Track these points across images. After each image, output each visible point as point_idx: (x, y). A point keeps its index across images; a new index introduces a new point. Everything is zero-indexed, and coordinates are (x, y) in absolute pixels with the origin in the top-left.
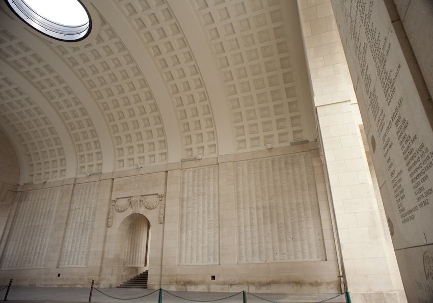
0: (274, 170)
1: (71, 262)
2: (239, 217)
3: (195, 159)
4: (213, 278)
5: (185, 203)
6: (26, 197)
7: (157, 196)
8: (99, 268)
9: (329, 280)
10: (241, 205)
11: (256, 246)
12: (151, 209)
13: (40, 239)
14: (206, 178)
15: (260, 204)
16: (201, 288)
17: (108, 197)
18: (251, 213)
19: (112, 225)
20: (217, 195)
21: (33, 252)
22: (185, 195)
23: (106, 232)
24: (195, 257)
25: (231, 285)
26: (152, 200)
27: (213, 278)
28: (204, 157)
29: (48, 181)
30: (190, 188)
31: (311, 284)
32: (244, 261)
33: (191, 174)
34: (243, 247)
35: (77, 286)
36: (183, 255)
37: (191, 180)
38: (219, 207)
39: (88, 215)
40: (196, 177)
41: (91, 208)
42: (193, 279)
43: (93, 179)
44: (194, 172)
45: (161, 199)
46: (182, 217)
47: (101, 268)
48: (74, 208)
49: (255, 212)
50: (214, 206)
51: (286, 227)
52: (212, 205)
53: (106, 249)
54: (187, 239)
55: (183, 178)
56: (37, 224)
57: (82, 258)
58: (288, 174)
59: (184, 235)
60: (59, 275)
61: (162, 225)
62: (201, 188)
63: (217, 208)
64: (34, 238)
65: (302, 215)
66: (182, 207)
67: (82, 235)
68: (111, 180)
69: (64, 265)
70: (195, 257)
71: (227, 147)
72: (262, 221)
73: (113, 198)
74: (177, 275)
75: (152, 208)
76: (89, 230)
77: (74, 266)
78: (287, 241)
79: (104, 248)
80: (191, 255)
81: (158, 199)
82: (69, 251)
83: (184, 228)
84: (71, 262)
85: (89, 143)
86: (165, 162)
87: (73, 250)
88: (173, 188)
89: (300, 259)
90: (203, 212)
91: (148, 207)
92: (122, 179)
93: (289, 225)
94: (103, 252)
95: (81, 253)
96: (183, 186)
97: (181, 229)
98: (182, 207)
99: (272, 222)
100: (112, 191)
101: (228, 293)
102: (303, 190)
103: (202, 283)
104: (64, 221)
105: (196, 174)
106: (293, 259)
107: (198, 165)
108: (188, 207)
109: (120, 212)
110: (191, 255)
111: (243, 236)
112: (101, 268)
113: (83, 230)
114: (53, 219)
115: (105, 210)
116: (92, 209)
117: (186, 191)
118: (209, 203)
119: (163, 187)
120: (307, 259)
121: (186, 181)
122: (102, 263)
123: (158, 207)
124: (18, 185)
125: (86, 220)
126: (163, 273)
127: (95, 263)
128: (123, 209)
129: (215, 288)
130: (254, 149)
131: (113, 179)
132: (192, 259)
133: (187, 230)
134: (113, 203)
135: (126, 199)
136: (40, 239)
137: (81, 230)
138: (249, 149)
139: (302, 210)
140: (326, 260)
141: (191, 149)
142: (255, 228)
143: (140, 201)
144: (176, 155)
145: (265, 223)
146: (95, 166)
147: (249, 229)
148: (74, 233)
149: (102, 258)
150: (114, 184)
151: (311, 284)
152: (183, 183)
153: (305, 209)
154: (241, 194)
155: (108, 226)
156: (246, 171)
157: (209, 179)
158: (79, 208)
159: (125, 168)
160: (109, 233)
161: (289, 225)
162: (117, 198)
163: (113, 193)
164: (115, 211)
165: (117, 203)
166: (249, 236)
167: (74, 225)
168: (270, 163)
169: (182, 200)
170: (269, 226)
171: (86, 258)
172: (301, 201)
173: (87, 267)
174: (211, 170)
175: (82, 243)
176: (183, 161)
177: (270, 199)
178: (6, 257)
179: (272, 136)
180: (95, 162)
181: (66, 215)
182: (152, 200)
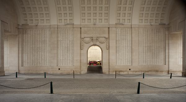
0: (152, 33)
1: (64, 64)
2: (139, 49)
3: (123, 24)
4: (130, 69)
5: (118, 42)
6: (26, 32)
9: (165, 70)
10: (140, 45)
11: (144, 59)
13: (43, 53)
14: (126, 32)
15: (147, 45)
16: (125, 73)
17: (79, 36)
18: (143, 48)
20: (131, 40)
21: (41, 59)
22: (118, 39)
23: (80, 52)
24: (122, 62)
25: (136, 72)
27: (130, 69)
28: (125, 24)
29: (40, 24)
30: (120, 36)
31: (161, 71)
32: (140, 64)
33: (120, 30)
34: (140, 59)
36: (118, 62)
37: (120, 33)
38: (132, 45)
39: (69, 44)
40: (122, 32)
42: (122, 70)
43: (68, 26)
44: (121, 30)
45: (107, 39)
46: (116, 47)
47: (80, 66)
48: (60, 40)
49: (144, 47)
50: (130, 44)
51: (155, 54)
52: (129, 44)
53: (82, 59)
55: (116, 32)
56: (38, 46)
57: (69, 62)
58: (157, 35)
59: (118, 54)
60: (59, 69)
61: (108, 50)
63: (131, 45)
64: (39, 53)
65: (160, 50)
66: (116, 44)
67: (67, 53)
69: (60, 65)
70: (122, 62)
71: (135, 21)
72: (147, 51)
73: (82, 37)
76: (71, 50)
77: (66, 65)
78: (154, 58)
80: (121, 62)
81: (105, 39)
84: (64, 64)
85: (66, 7)
86: (108, 23)
87: (64, 59)
88: (112, 35)
89: (158, 64)
93: (156, 53)
94: (81, 60)
95: (68, 60)
96: (116, 35)
98: (116, 44)
99: (150, 52)
101: (135, 74)
102: (161, 42)
103: (126, 71)
104: (56, 46)
105: (122, 31)
106: (156, 64)
107: (123, 27)
110: (121, 62)
111: (140, 56)
113: (67, 51)
114: (48, 45)
116: (71, 41)
117: (118, 37)
118: (127, 43)
120: (160, 64)
121: (118, 33)
122: (80, 64)
123: (106, 43)
124: (19, 25)
125: (68, 46)
126: (110, 68)
127: (77, 64)
129: (130, 73)
130: (145, 24)
131: (81, 28)
132: (121, 63)
136: (43, 53)
138: (143, 24)
139: (160, 49)
140: (165, 64)
141: (119, 19)
142: (145, 53)
144: (113, 21)
145: (148, 52)
147: (142, 54)
148: (62, 51)
149: (80, 63)
150: (82, 30)
151: (161, 71)
153: (161, 49)
154: (140, 41)
155: (81, 49)
156: (142, 32)
157: (127, 33)
159: (86, 23)
161: (156, 53)
163: (82, 34)
166: (142, 56)
167: (62, 47)
168: (151, 30)
169: (116, 41)
170: (149, 53)
172: (160, 45)
174: (129, 30)
175: (68, 56)
176: (116, 24)
177: (150, 44)
178: (24, 60)
179: (153, 19)
180: (68, 18)
181: (56, 43)
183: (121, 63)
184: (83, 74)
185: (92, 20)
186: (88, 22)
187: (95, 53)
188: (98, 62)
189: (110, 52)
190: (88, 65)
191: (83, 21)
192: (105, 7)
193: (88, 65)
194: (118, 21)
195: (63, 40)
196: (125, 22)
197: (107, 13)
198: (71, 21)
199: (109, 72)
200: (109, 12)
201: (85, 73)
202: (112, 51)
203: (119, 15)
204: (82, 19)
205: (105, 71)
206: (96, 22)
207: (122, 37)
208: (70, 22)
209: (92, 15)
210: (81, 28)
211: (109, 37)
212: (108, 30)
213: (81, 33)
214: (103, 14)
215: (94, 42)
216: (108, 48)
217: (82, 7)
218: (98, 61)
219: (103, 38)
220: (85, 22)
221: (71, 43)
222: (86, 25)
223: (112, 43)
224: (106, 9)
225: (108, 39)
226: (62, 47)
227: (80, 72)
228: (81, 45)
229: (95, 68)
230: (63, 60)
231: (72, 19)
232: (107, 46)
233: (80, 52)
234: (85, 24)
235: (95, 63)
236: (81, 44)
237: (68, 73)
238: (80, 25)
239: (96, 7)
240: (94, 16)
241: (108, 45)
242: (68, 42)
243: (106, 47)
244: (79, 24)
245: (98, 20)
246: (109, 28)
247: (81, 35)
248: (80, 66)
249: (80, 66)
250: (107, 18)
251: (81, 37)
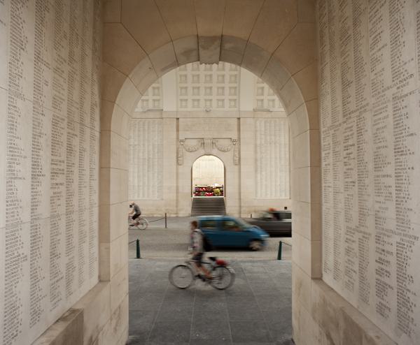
1: (141, 195)
8: (175, 202)
20: (288, 146)
22: (258, 142)
23: (177, 169)
26: (226, 143)
30: (263, 136)
33: (263, 124)
35: (155, 216)
37: (263, 129)
41: (153, 145)
43: (151, 115)
46: (256, 160)
47: (177, 201)
48: (132, 144)
50: (285, 154)
54: (261, 179)
55: (256, 127)
59: (259, 175)
61: (237, 167)
62: (273, 137)
66: (256, 152)
67: (148, 171)
74: (255, 206)
79: (177, 183)
81: (231, 143)
82: (136, 185)
83: (259, 170)
84: (141, 195)
90: (276, 158)
92: (189, 119)
94: (177, 187)
97: (256, 171)
100: (178, 130)
108: (261, 153)
115: (174, 148)
118: (280, 151)
119: (236, 133)
122: (177, 197)
125: (151, 156)
126: (242, 205)
131: (178, 119)
132: (266, 194)
133: (261, 171)
137: (146, 168)
141: (262, 100)
146: (151, 101)
149: (177, 192)
150: (180, 123)
152: (256, 131)
155: (178, 164)
158: (139, 145)
159: (190, 108)
160: (180, 171)
164: (184, 150)
167: (136, 160)
171: (158, 192)
173: (163, 199)
176: (255, 110)
182: (226, 143)
183: (266, 194)
184: (184, 217)
185: (202, 103)
186: (194, 107)
187: (208, 170)
188: (217, 188)
189: (242, 170)
190: (194, 195)
191: (184, 103)
192: (231, 76)
193: (194, 195)
194: (260, 103)
195: (139, 145)
196: (274, 107)
197: (235, 100)
198: (156, 103)
199: (240, 213)
200: (239, 85)
201: (187, 215)
202: (247, 167)
203: (260, 91)
204: (181, 100)
206: (211, 106)
207: (268, 138)
208: (154, 106)
209: (202, 91)
210: (178, 119)
211: (239, 138)
212: (236, 123)
213: (178, 130)
214: (227, 91)
215: (207, 146)
216: (238, 163)
217: (181, 76)
218: (216, 185)
220: (186, 107)
221: (156, 150)
222: (190, 112)
223: (247, 152)
224: (233, 78)
225: (237, 142)
226: (136, 160)
227: (177, 214)
230: (138, 186)
231: (159, 100)
232: (235, 158)
233: (175, 171)
234: (185, 109)
235: (210, 190)
236: (177, 153)
237: (151, 216)
238: (177, 112)
239: (211, 88)
240: (206, 95)
241: (237, 156)
242: (151, 147)
243: (232, 161)
244: (175, 110)
245: (214, 103)
246: (239, 119)
247: (178, 135)
248: (177, 200)
249: (177, 200)
250: (235, 97)
251: (178, 138)
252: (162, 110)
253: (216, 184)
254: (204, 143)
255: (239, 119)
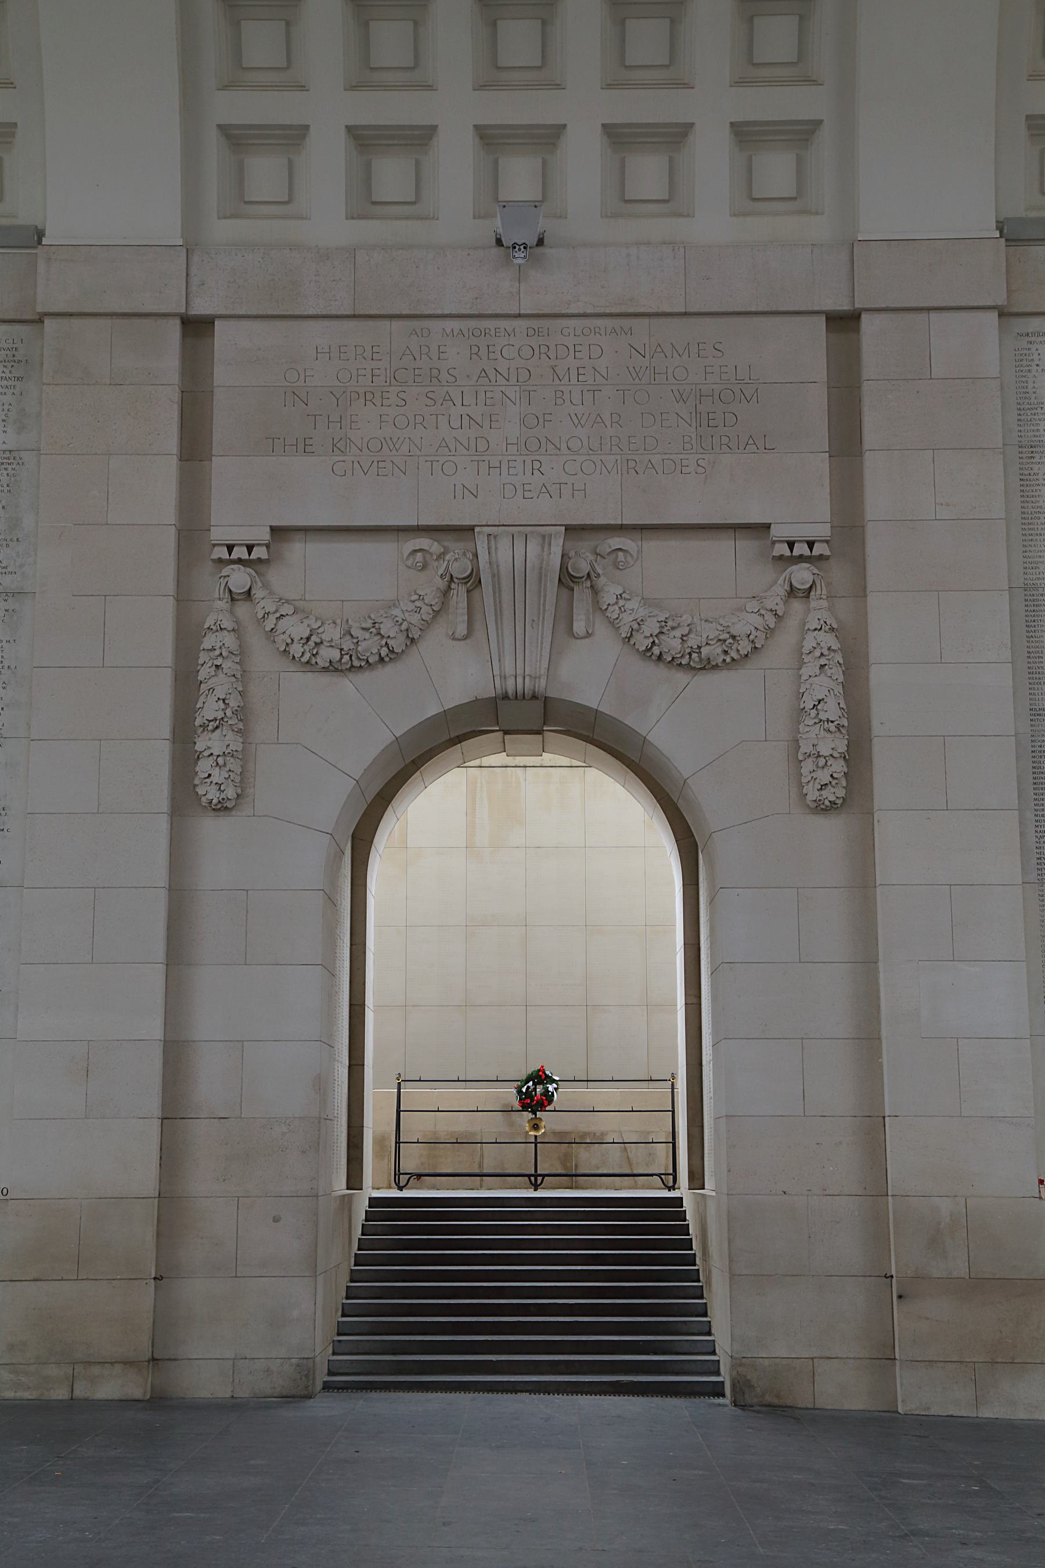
7: (747, 545)
12: (709, 666)
19: (243, 782)
26: (707, 586)
45: (802, 575)
53: (209, 1023)
61: (829, 833)
68: (174, 328)
73: (233, 521)
75: (714, 651)
91: (672, 644)
92: (315, 334)
94: (176, 1055)
109: (332, 668)
112: (170, 1208)
122: (171, 1158)
128: (370, 646)
131: (196, 328)
134: (239, 578)
135: (385, 550)
143: (567, 579)
149: (173, 1114)
150: (222, 375)
162: (273, 529)
165: (275, 576)
182: (707, 586)
199: (884, 1358)
205: (781, 1350)
210: (196, 328)
211: (850, 527)
213: (194, 446)
219: (724, 547)
223: (938, 666)
228: (209, 709)
229: (523, 1281)
236: (186, 685)
241: (832, 710)
245: (583, 160)
246: (844, 323)
252: (40, 234)
253: (623, 1125)
254: (473, 581)
255: (844, 323)
